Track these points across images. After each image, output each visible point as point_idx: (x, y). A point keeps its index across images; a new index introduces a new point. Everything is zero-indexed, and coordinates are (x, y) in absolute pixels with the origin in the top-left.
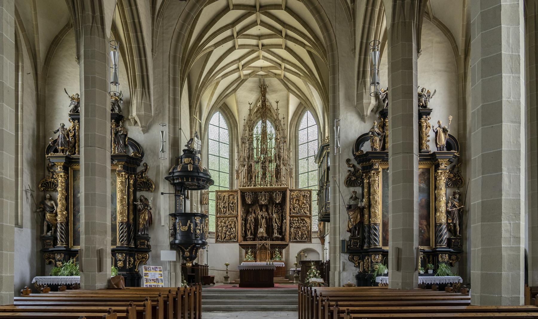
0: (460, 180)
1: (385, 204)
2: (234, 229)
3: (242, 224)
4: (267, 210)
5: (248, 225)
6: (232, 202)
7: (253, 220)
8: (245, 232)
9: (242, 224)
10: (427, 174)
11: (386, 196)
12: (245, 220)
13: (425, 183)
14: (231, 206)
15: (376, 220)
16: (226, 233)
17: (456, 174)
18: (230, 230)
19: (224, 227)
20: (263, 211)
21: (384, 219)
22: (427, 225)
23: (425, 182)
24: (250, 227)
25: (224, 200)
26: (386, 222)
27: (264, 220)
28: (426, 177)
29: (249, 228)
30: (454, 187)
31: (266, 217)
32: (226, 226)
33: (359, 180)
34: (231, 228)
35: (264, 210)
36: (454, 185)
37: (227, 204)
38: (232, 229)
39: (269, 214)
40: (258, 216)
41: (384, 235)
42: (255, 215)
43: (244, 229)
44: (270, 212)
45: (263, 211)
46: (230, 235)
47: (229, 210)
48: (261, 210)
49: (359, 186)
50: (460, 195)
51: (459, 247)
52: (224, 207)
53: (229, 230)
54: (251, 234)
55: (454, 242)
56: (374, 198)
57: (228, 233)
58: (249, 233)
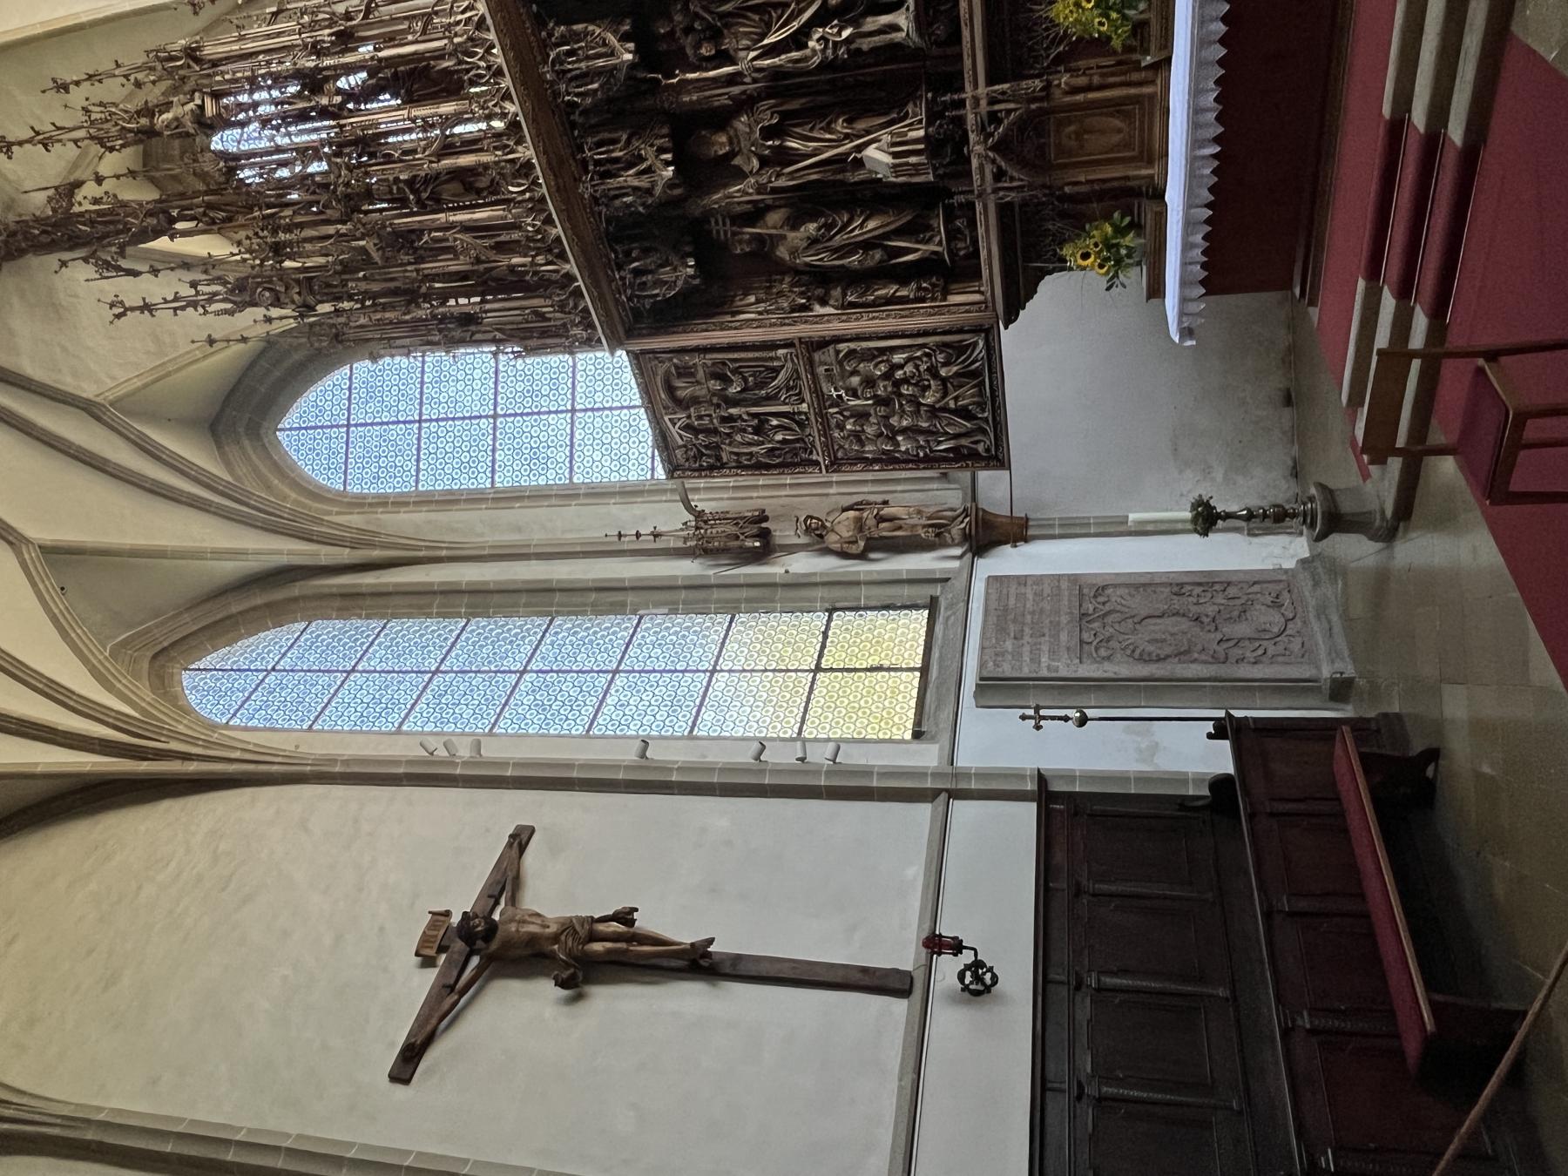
2: (898, 358)
3: (852, 305)
4: (721, 119)
5: (854, 260)
6: (715, 385)
7: (812, 227)
8: (903, 275)
9: (852, 305)
12: (820, 282)
14: (743, 391)
16: (933, 411)
18: (906, 381)
19: (894, 421)
20: (732, 155)
24: (867, 245)
25: (715, 432)
27: (792, 144)
29: (878, 255)
31: (768, 133)
32: (882, 411)
34: (887, 376)
35: (720, 143)
37: (733, 411)
38: (899, 374)
39: (745, 104)
40: (775, 190)
42: (769, 208)
43: (890, 290)
44: (722, 97)
45: (732, 155)
46: (944, 381)
47: (770, 399)
48: (725, 170)
52: (757, 430)
53: (905, 390)
54: (915, 230)
57: (929, 399)
58: (915, 251)
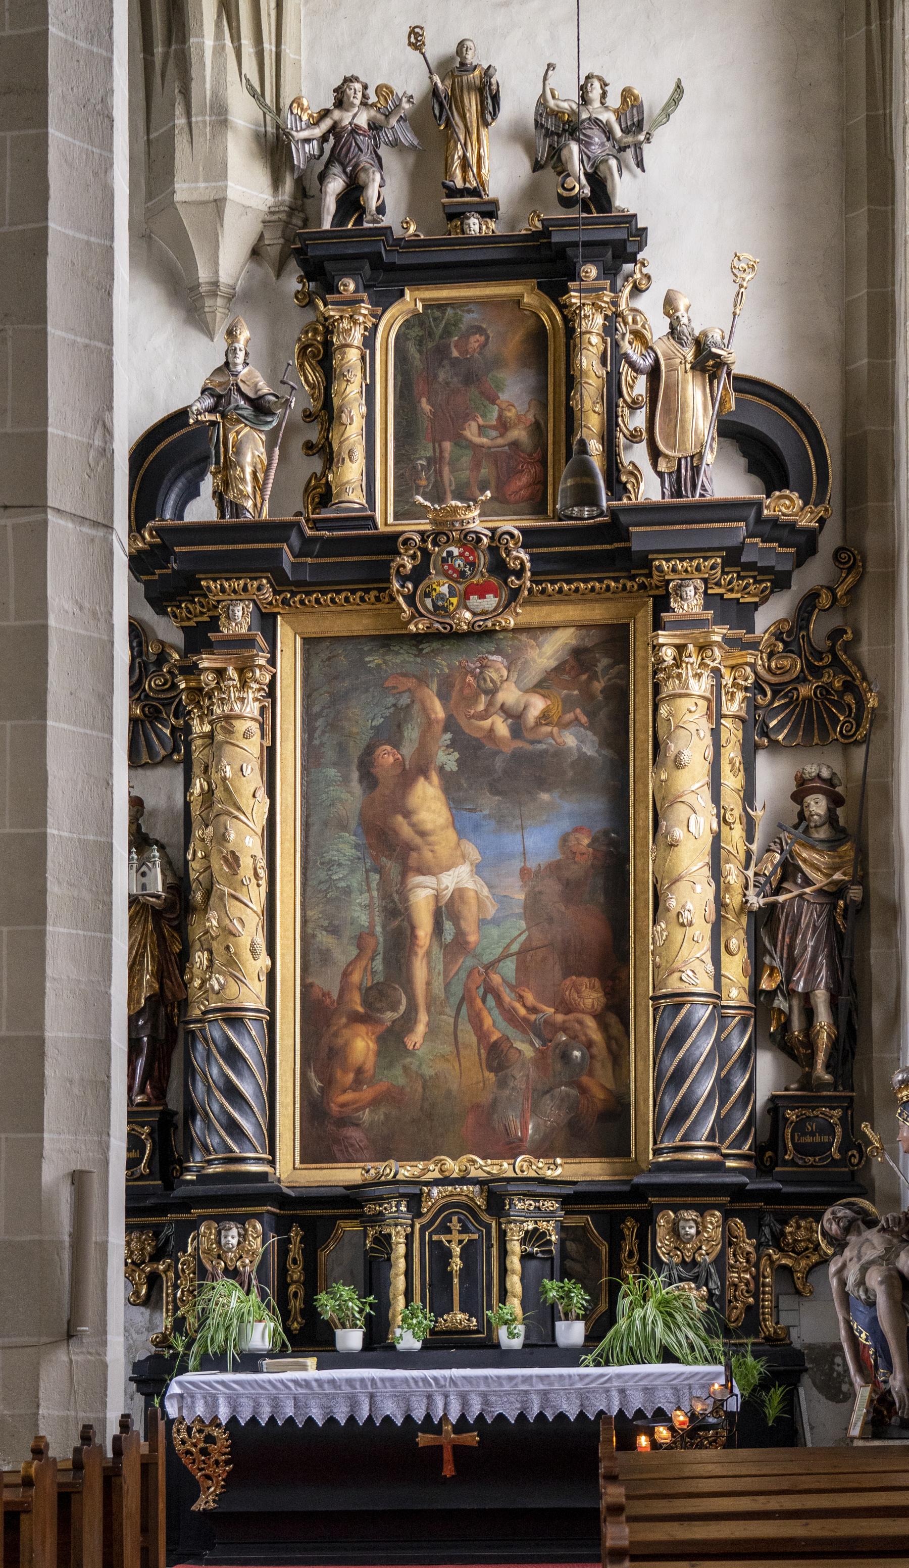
0: (849, 699)
1: (323, 875)
10: (604, 662)
11: (325, 824)
13: (591, 727)
15: (233, 988)
17: (819, 655)
21: (319, 981)
22: (608, 1007)
23: (592, 715)
26: (327, 994)
28: (598, 686)
30: (807, 744)
33: (164, 722)
36: (808, 732)
41: (316, 1084)
49: (166, 760)
50: (835, 800)
51: (834, 1163)
55: (800, 1127)
56: (222, 838)
